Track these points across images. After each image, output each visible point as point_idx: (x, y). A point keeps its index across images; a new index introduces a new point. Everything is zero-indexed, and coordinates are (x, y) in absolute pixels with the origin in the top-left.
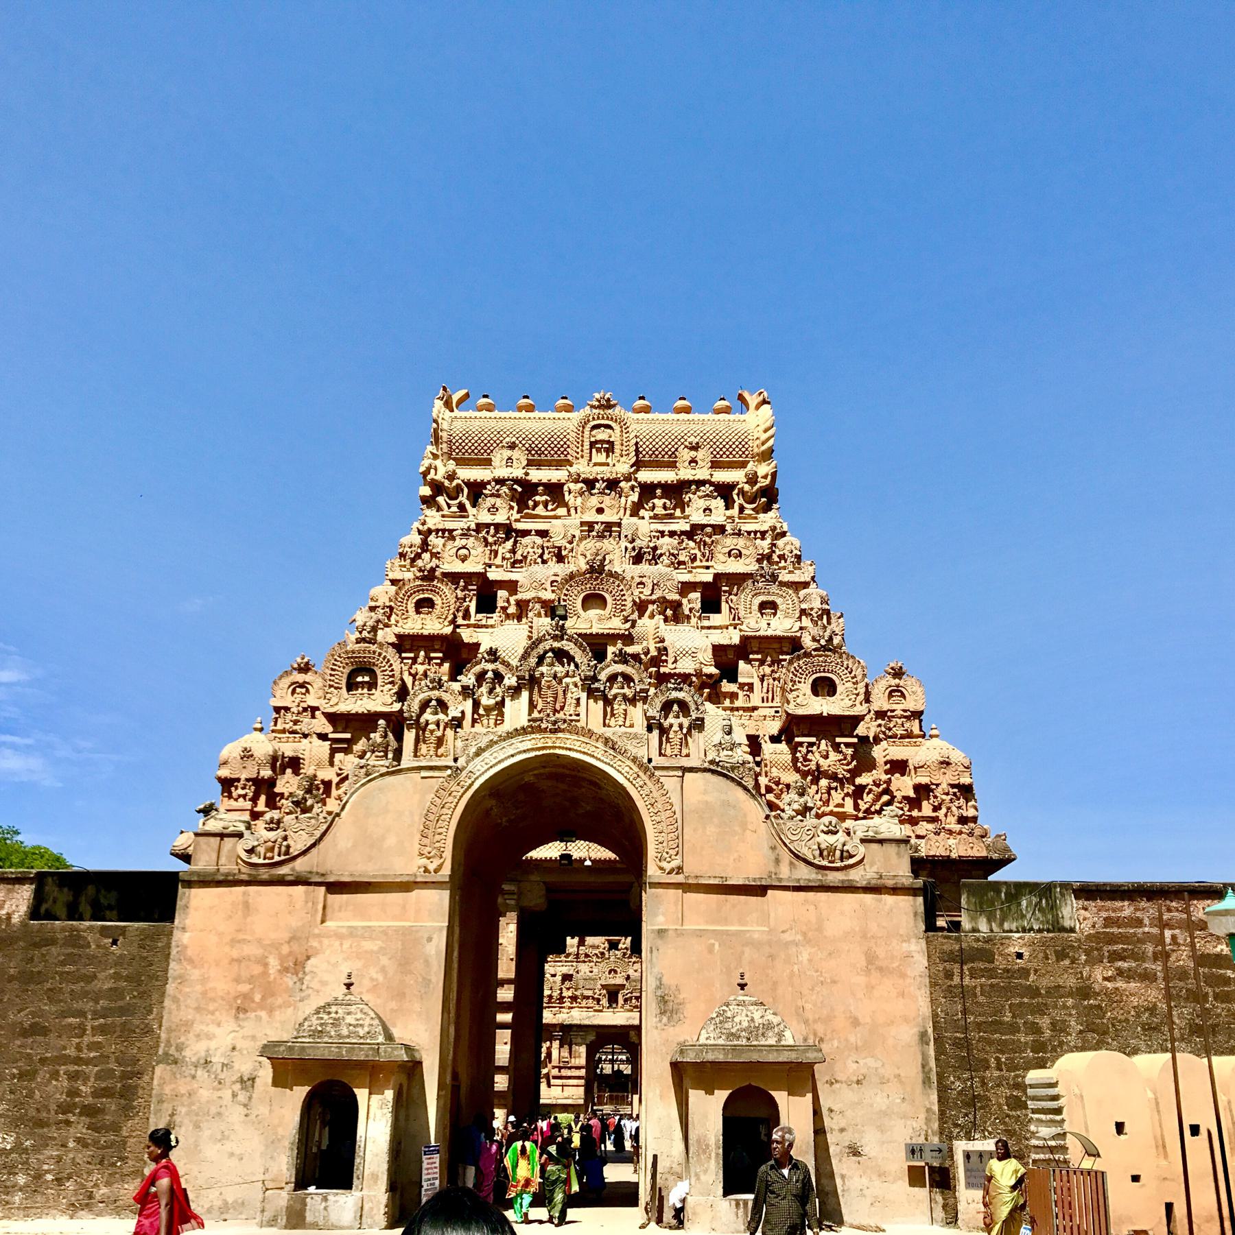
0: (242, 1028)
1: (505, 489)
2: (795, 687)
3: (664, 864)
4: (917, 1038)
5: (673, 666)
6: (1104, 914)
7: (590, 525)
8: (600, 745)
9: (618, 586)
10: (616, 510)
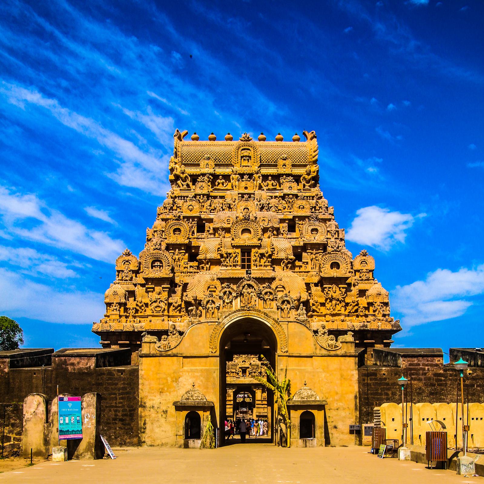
0: (162, 397)
1: (206, 178)
2: (324, 266)
3: (283, 350)
4: (354, 397)
5: (277, 256)
6: (409, 362)
7: (243, 195)
8: (263, 315)
9: (256, 226)
10: (253, 188)
